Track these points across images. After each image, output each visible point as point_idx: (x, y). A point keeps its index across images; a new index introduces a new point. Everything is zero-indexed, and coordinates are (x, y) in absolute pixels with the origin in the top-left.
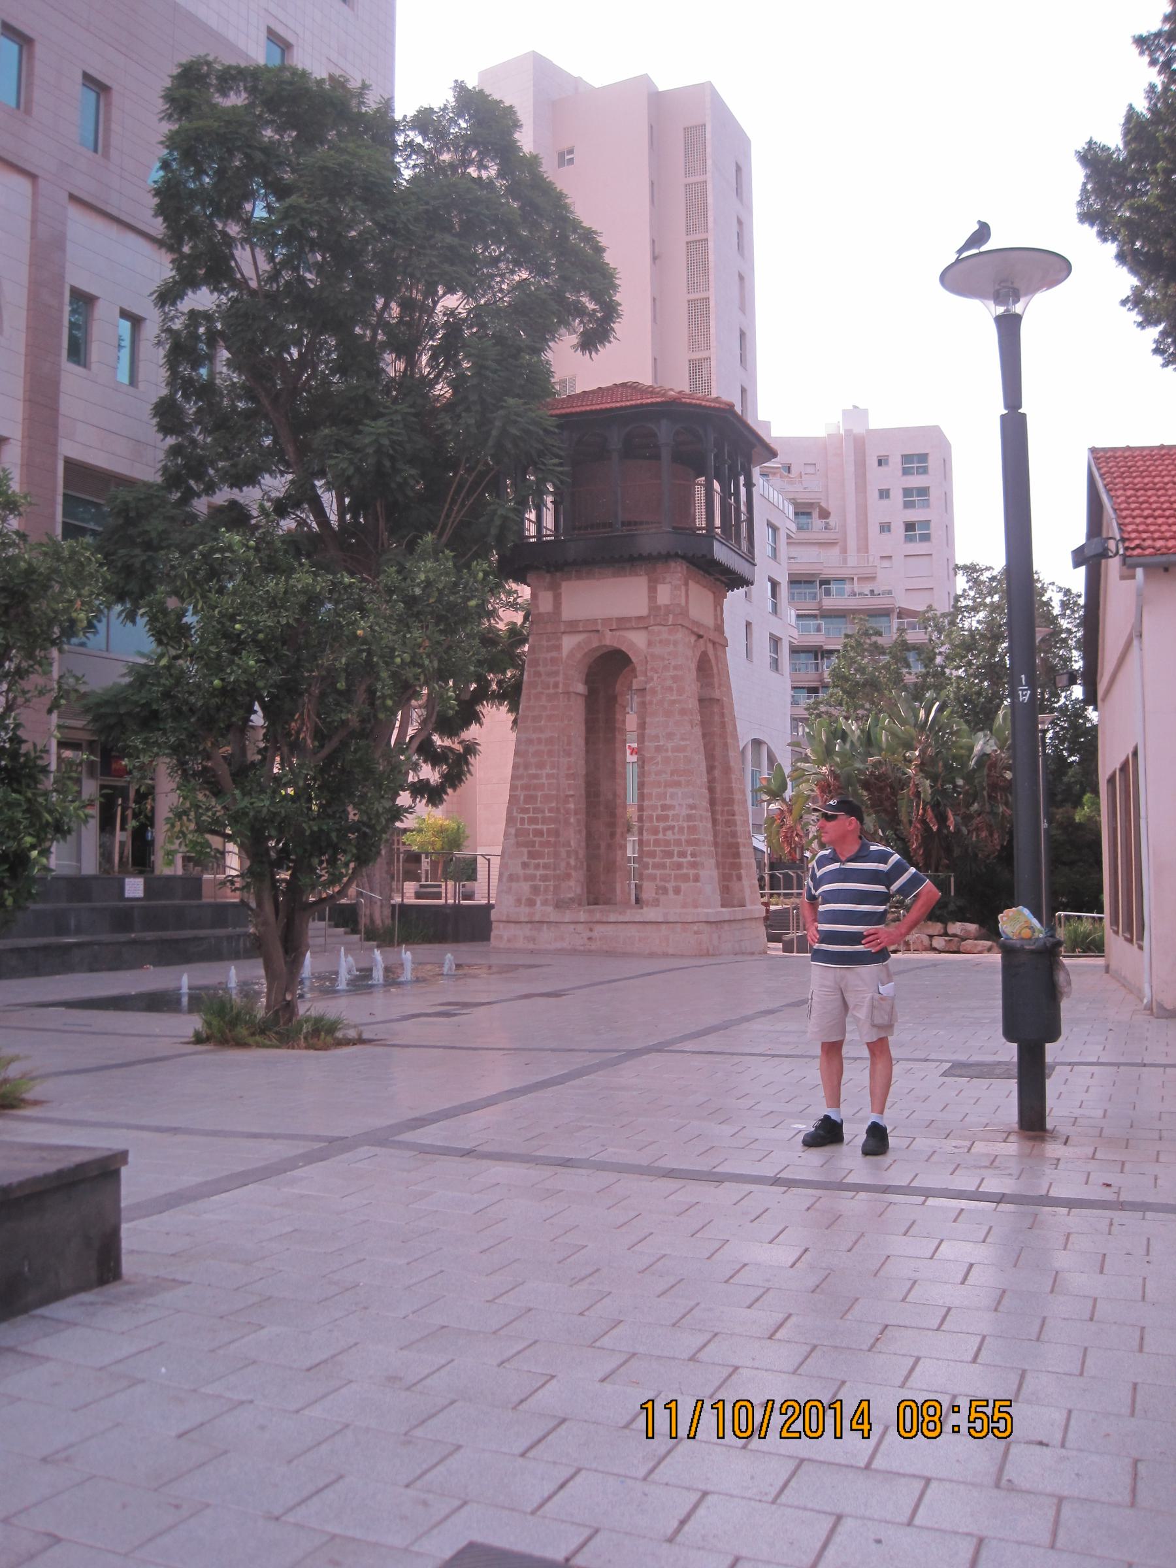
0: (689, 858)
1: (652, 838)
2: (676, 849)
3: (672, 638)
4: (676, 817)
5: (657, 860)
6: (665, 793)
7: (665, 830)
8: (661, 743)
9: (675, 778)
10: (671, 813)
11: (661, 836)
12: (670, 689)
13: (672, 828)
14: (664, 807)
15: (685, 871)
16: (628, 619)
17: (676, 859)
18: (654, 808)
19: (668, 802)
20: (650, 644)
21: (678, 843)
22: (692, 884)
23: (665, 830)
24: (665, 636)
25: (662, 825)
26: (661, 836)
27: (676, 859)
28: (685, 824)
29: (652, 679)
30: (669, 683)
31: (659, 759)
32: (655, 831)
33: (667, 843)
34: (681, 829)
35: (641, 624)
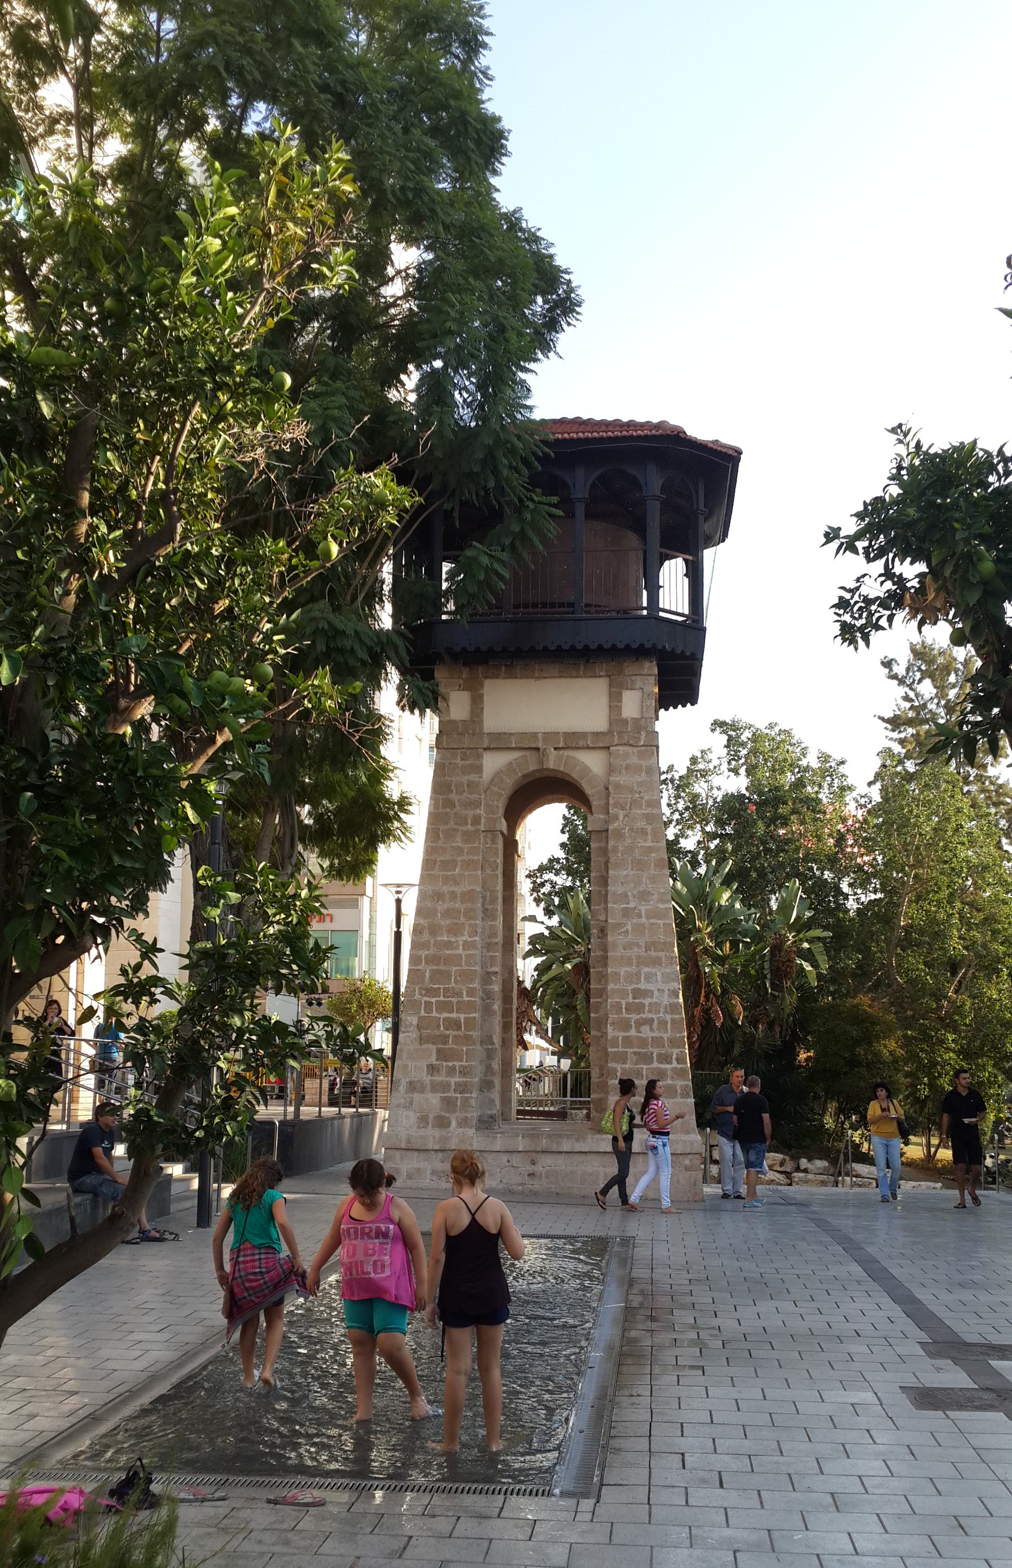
0: (675, 1064)
1: (621, 1035)
2: (656, 1052)
3: (644, 763)
4: (655, 1007)
5: (627, 1066)
6: (638, 975)
7: (639, 1023)
8: (632, 905)
9: (652, 953)
10: (647, 1001)
11: (633, 1032)
12: (643, 832)
13: (649, 1022)
14: (638, 993)
15: (669, 1082)
16: (584, 735)
17: (655, 1064)
18: (623, 993)
19: (643, 986)
20: (611, 769)
21: (658, 1042)
22: (679, 1100)
23: (639, 1023)
24: (634, 760)
25: (634, 1017)
26: (633, 1032)
27: (655, 1064)
28: (668, 1017)
29: (616, 817)
30: (641, 824)
31: (629, 928)
32: (625, 1026)
33: (643, 1042)
34: (663, 1023)
35: (598, 742)
